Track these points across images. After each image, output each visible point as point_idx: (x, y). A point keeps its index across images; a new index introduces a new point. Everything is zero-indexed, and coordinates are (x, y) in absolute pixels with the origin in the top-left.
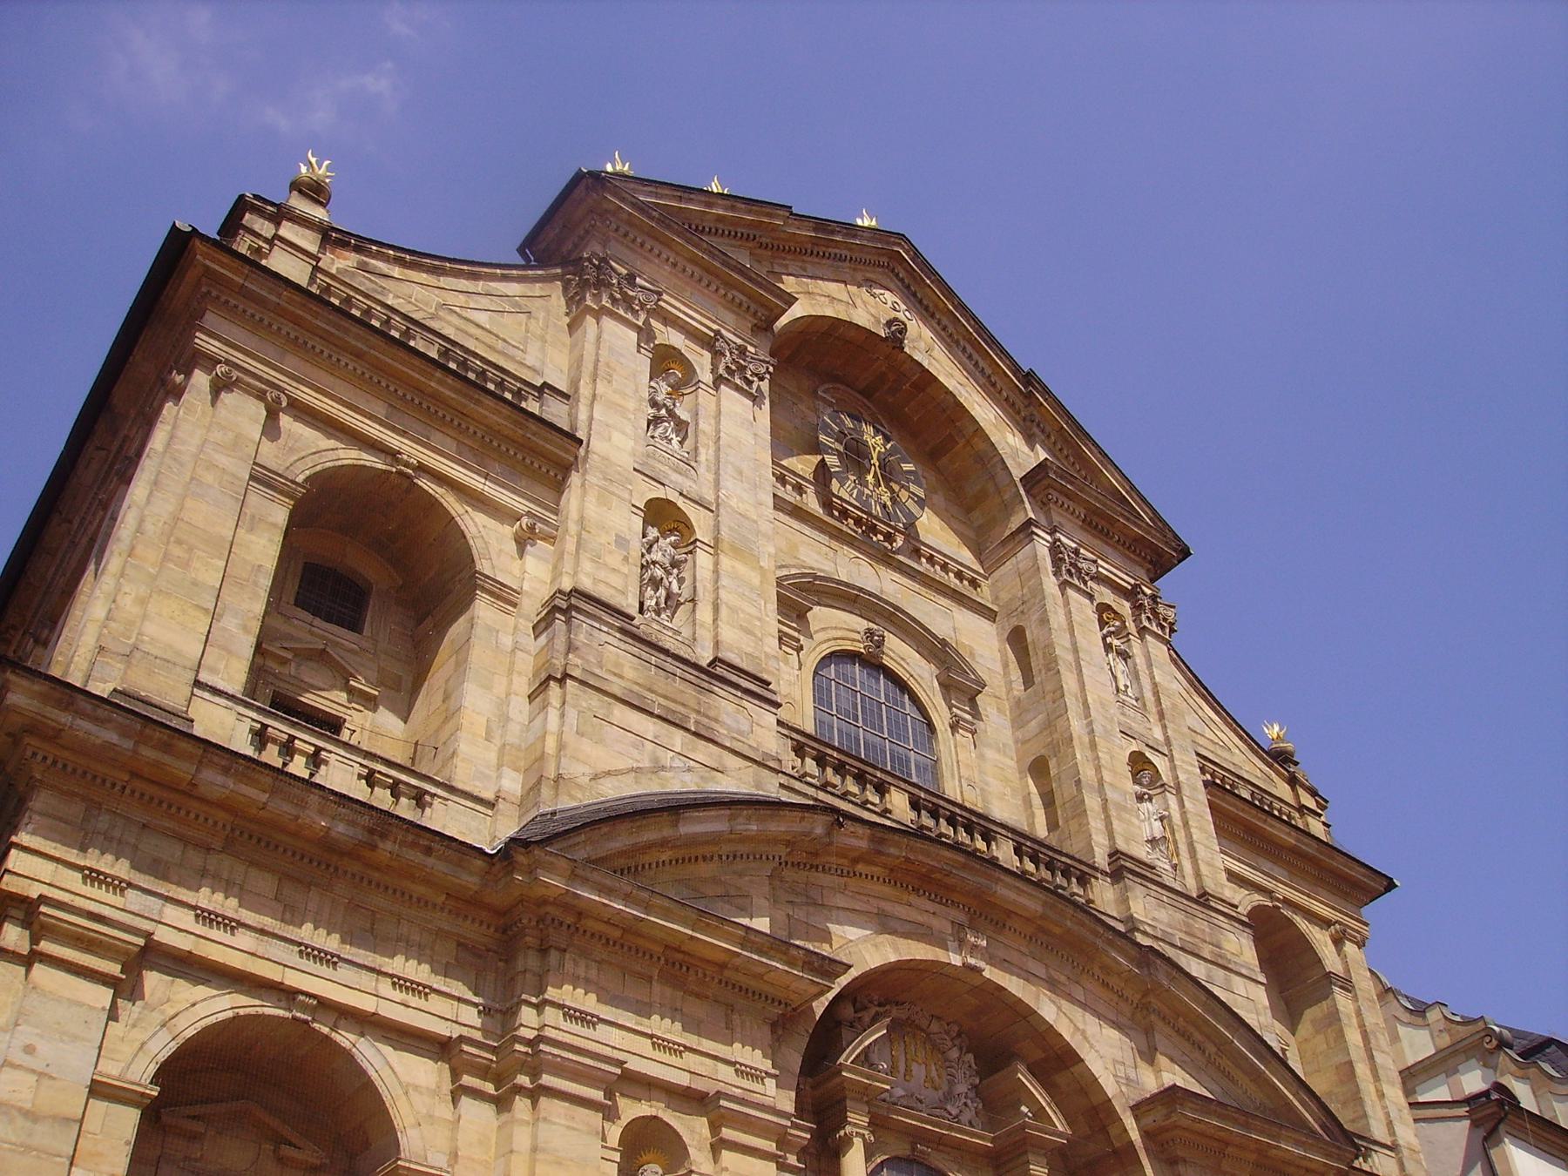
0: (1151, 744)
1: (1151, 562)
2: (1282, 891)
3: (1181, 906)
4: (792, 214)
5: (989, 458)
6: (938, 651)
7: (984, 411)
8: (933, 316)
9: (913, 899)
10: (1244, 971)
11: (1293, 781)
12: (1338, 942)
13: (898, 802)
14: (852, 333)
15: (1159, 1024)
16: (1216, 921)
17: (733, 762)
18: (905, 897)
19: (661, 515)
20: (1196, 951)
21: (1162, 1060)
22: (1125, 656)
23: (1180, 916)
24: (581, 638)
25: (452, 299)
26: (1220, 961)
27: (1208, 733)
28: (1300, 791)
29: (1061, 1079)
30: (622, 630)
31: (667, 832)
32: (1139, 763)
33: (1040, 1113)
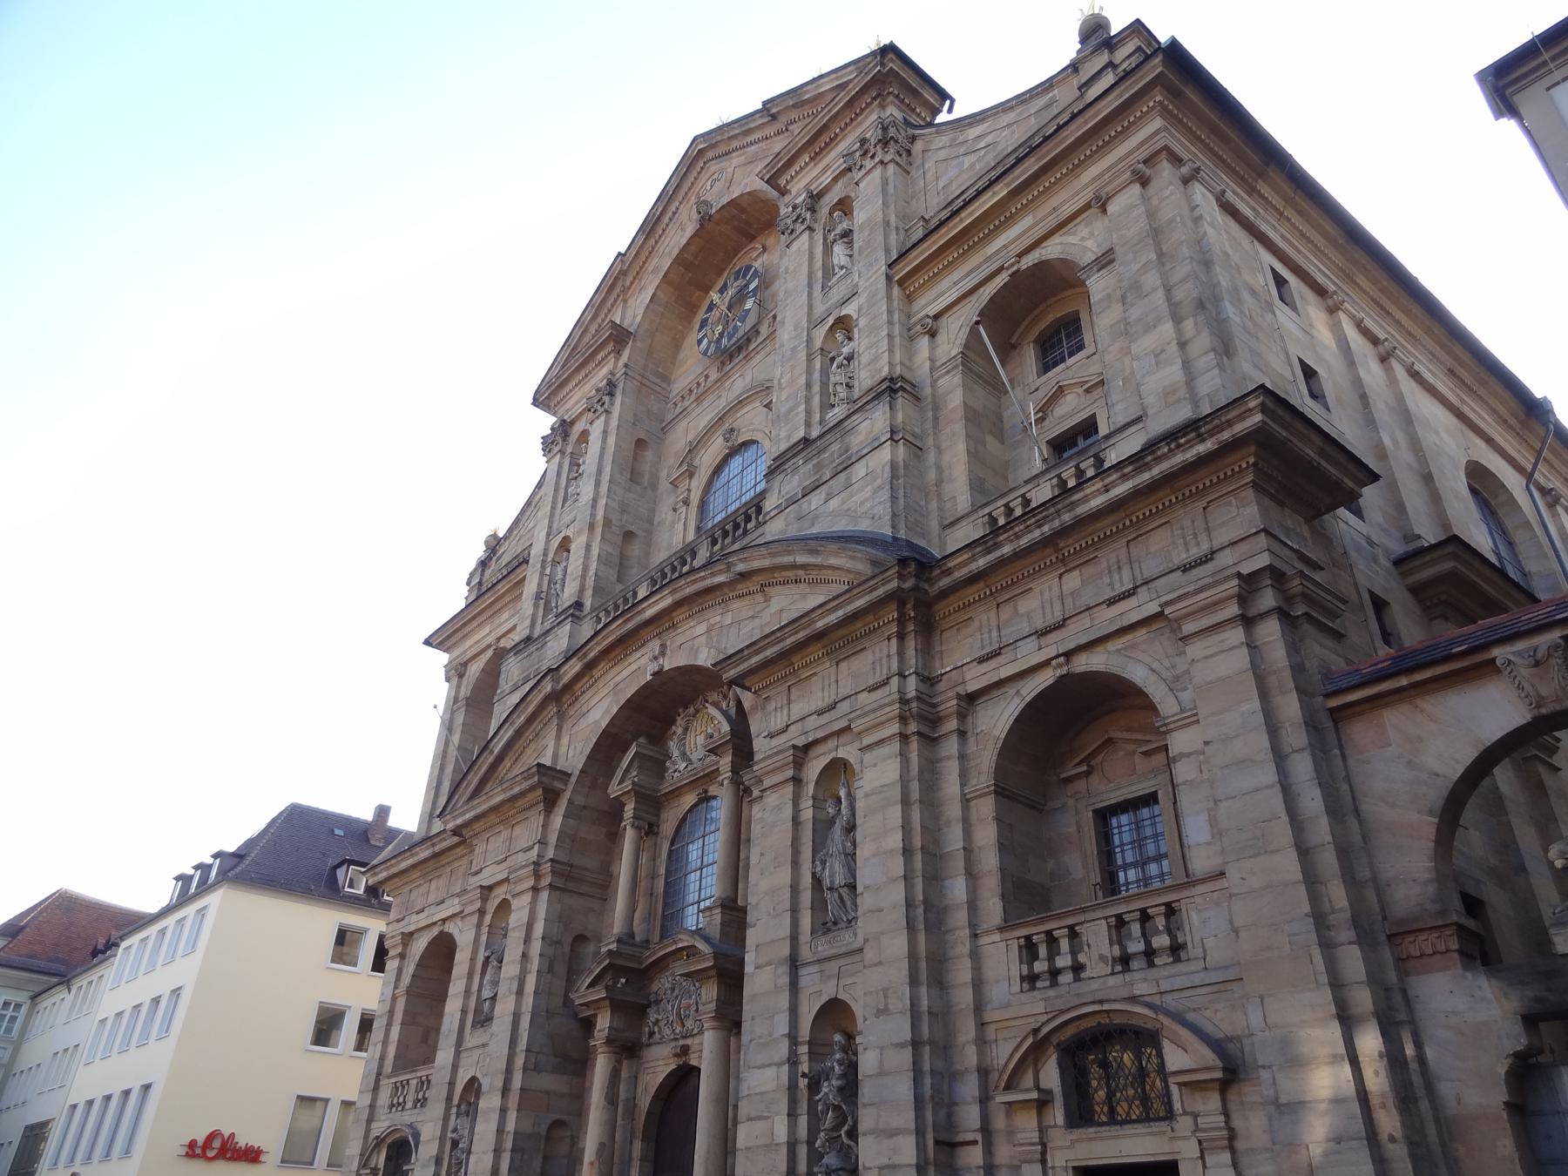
0: (845, 299)
1: (874, 99)
3: (814, 452)
4: (624, 255)
8: (730, 153)
9: (631, 659)
10: (865, 451)
14: (693, 248)
16: (850, 427)
18: (627, 663)
20: (817, 484)
23: (810, 466)
26: (841, 468)
27: (968, 160)
30: (515, 654)
31: (491, 759)
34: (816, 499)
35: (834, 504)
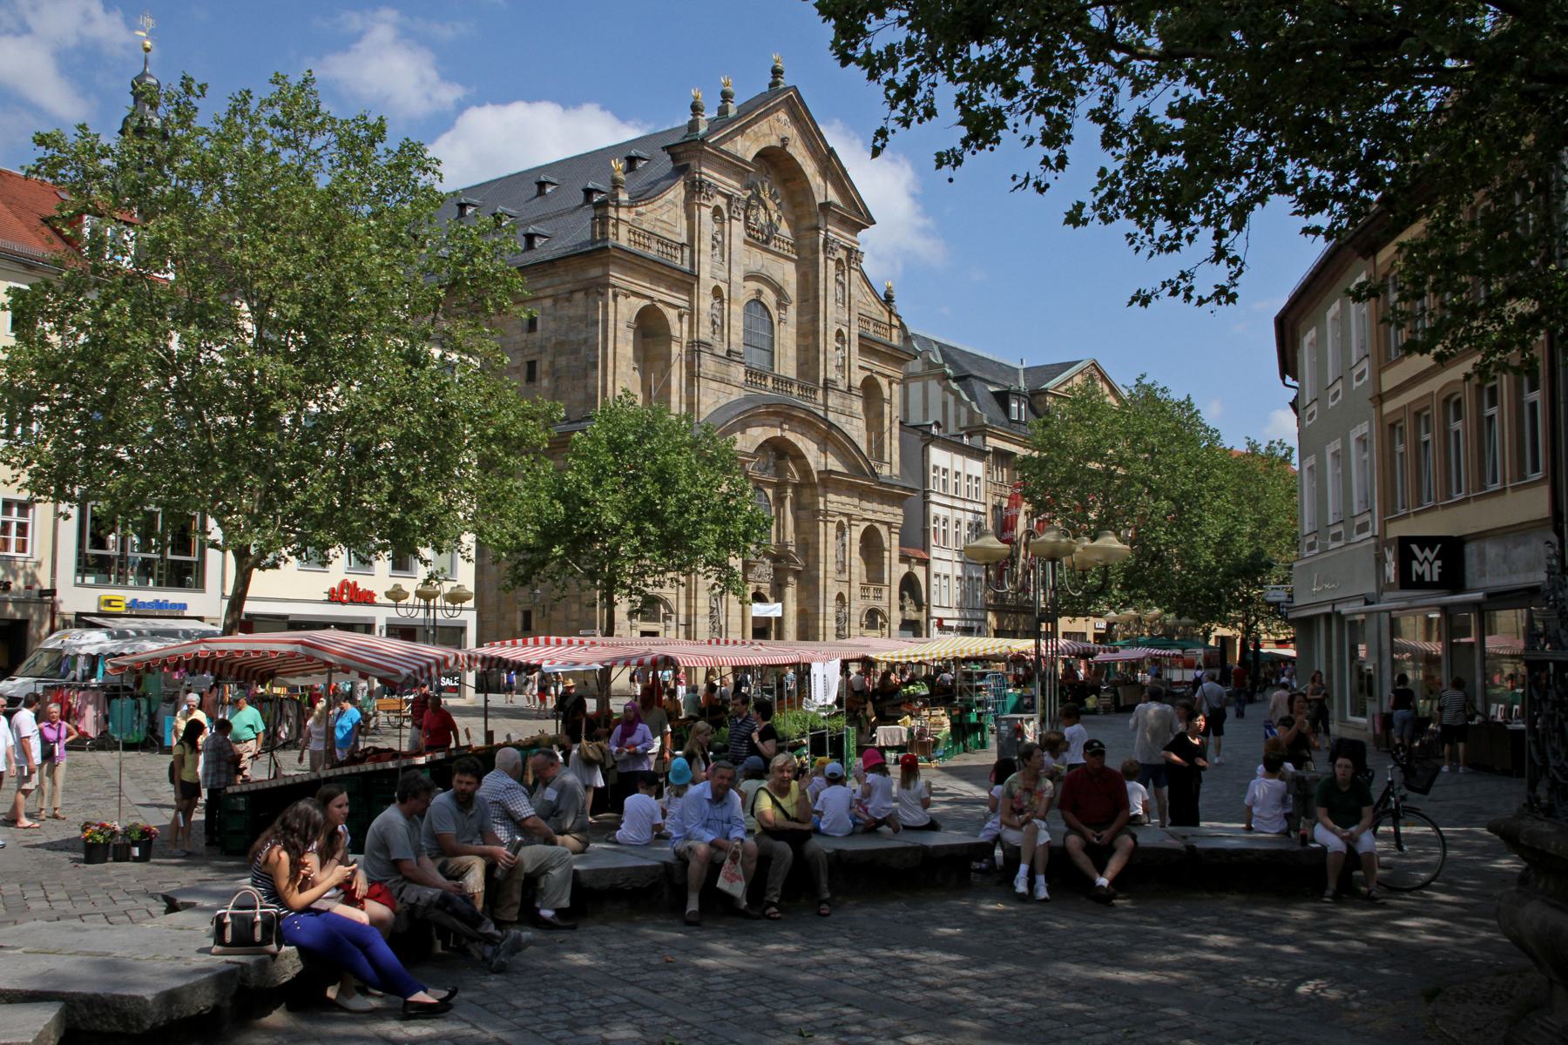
2: (876, 369)
5: (807, 190)
6: (779, 291)
7: (810, 168)
11: (891, 312)
12: (890, 384)
13: (770, 380)
15: (830, 443)
17: (735, 389)
19: (717, 292)
21: (829, 454)
22: (842, 284)
24: (702, 361)
25: (657, 214)
28: (893, 317)
29: (799, 461)
32: (839, 333)
33: (792, 473)
34: (843, 419)
35: (848, 427)
